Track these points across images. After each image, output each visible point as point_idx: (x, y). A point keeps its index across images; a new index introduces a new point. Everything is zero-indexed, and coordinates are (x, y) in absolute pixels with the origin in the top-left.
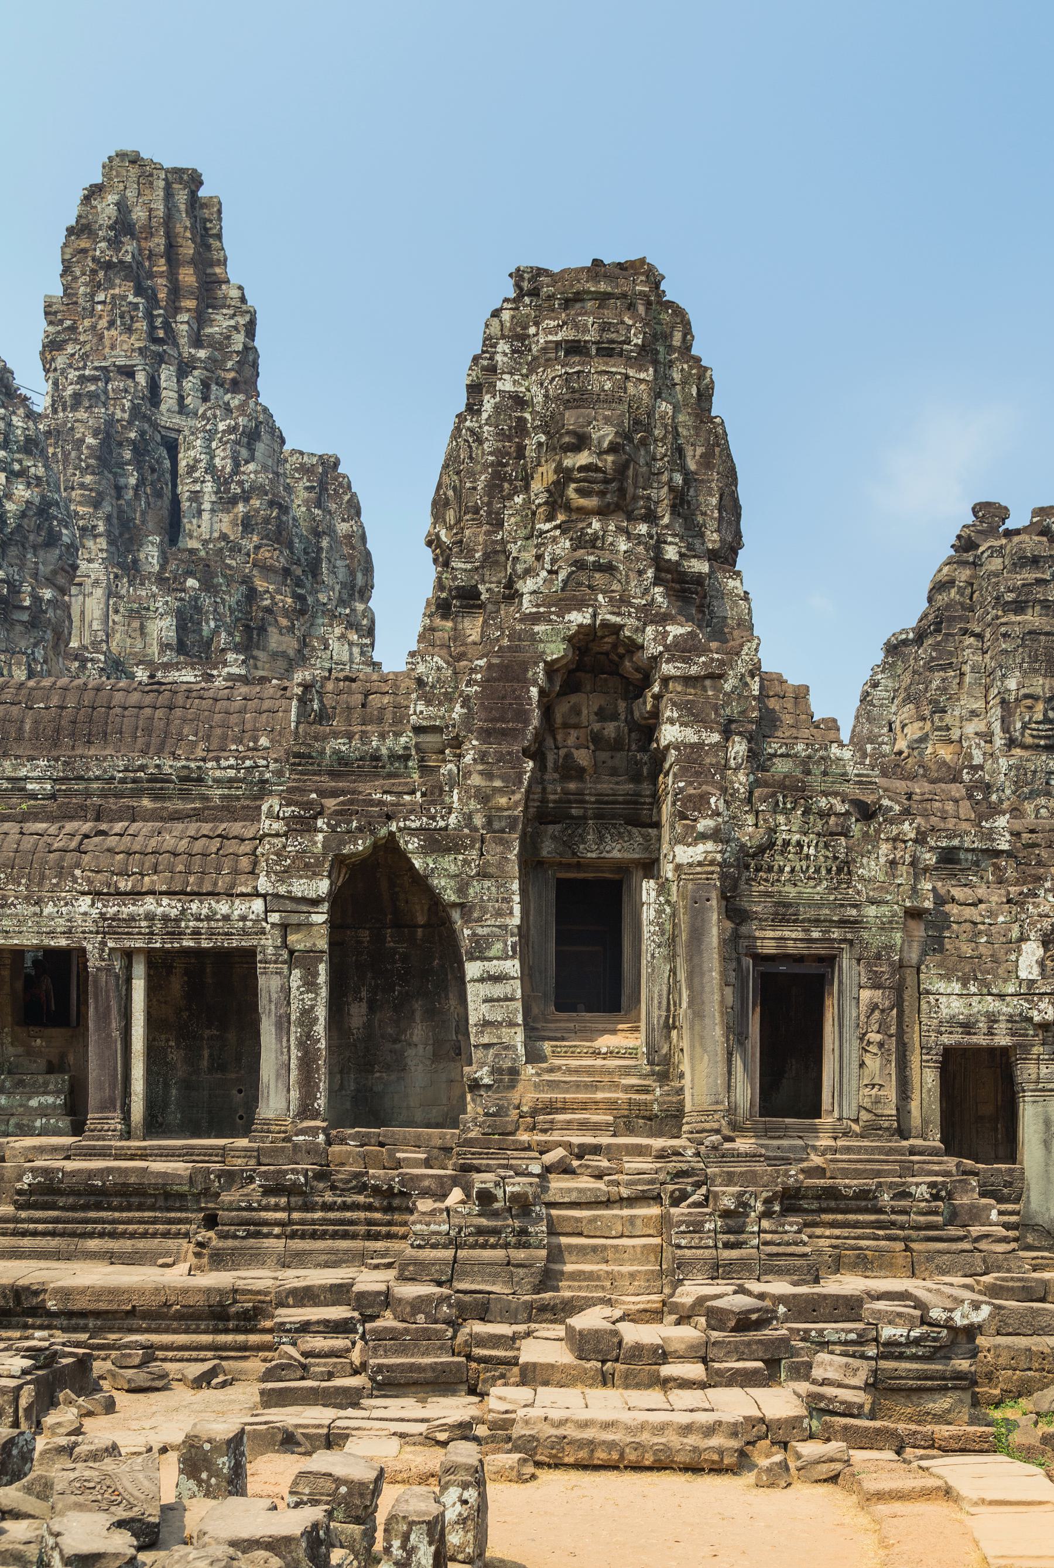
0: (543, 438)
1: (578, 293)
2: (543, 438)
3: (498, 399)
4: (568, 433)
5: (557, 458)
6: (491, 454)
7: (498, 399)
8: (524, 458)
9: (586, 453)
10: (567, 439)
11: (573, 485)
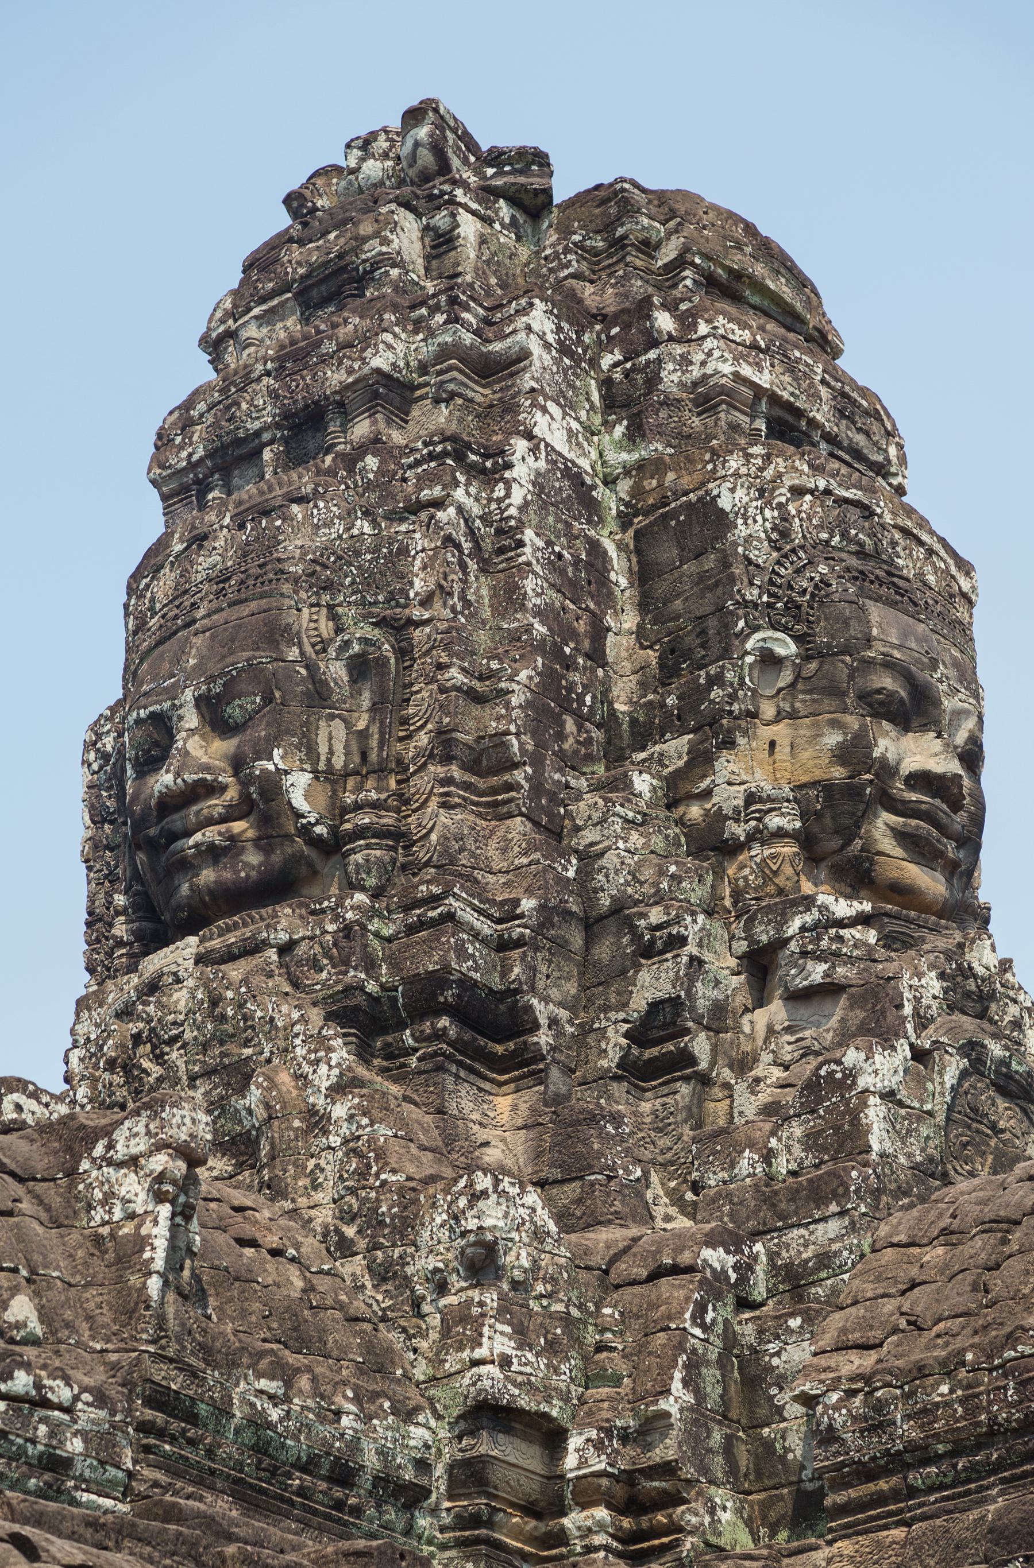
0: (786, 647)
1: (738, 275)
2: (786, 647)
3: (542, 464)
4: (889, 665)
5: (853, 722)
6: (538, 613)
7: (542, 464)
8: (604, 664)
9: (930, 742)
10: (887, 682)
11: (886, 818)
